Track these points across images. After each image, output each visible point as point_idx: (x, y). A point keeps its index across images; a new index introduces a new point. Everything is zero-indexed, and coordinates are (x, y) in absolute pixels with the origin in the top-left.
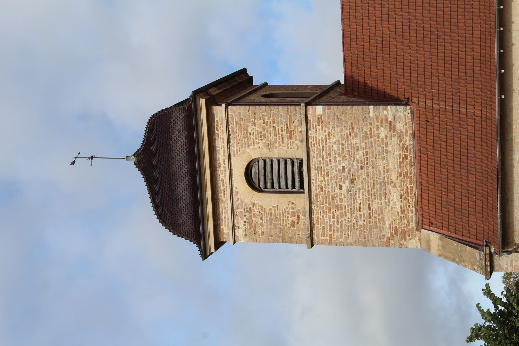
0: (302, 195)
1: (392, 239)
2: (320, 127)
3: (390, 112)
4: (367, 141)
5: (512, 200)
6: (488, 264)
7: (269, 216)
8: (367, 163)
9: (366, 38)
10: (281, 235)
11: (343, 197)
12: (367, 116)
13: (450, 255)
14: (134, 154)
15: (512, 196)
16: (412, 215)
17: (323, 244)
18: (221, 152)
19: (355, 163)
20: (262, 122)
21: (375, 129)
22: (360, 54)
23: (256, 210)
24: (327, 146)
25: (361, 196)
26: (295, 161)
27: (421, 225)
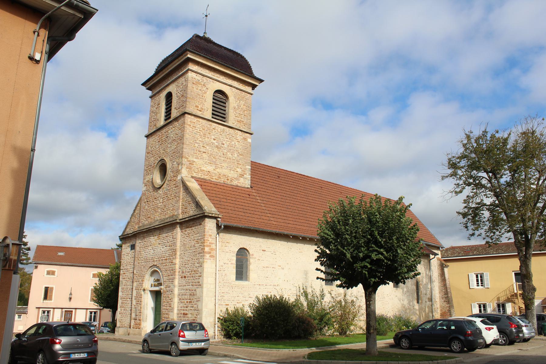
2: (242, 138)
3: (248, 176)
4: (235, 161)
5: (241, 235)
6: (213, 215)
7: (201, 95)
11: (210, 139)
12: (246, 164)
15: (243, 235)
18: (232, 83)
20: (245, 110)
23: (205, 89)
25: (210, 149)
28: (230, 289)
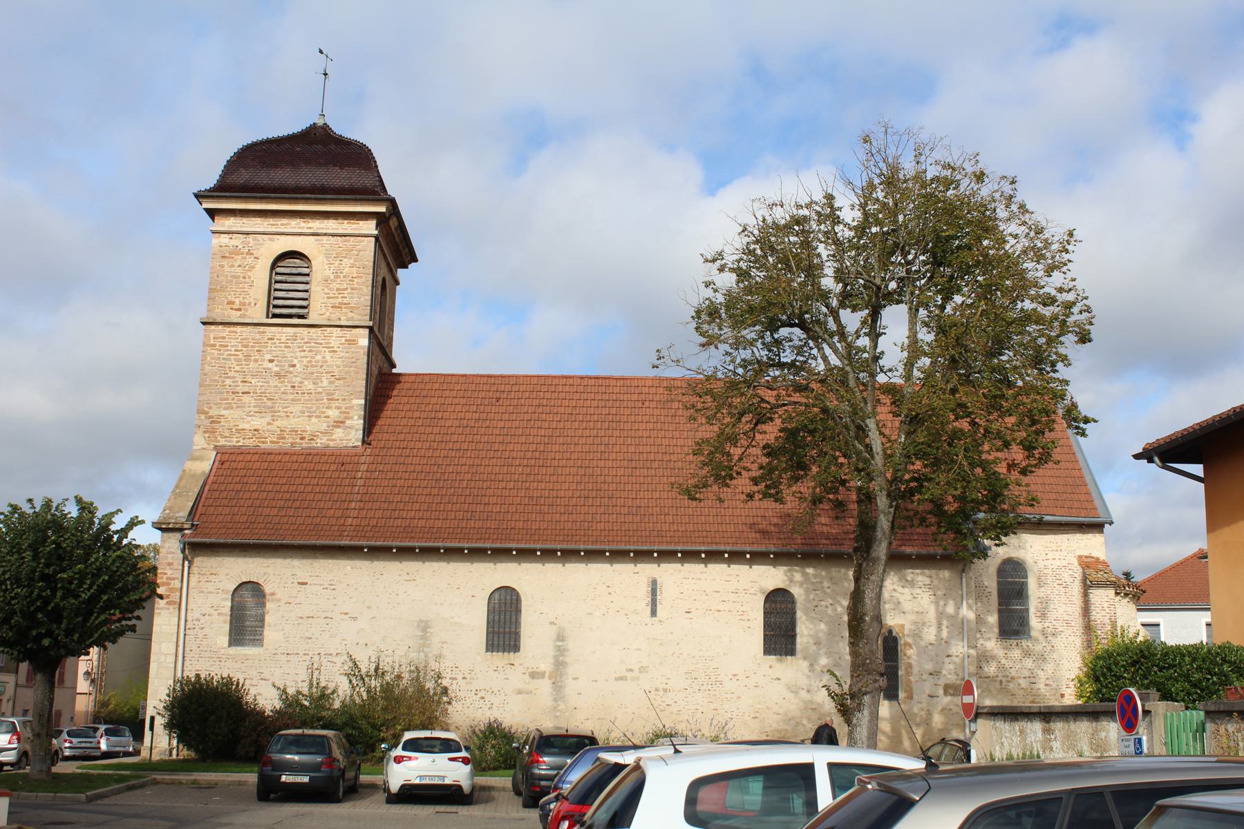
0: (265, 315)
1: (206, 417)
3: (356, 422)
5: (245, 556)
6: (171, 526)
7: (242, 275)
8: (298, 393)
9: (441, 401)
10: (218, 288)
12: (352, 397)
13: (183, 482)
14: (326, 124)
15: (250, 557)
16: (234, 442)
17: (205, 336)
18: (322, 225)
19: (298, 379)
20: (354, 276)
21: (337, 405)
22: (425, 393)
23: (250, 260)
24: (321, 349)
26: (306, 311)
27: (220, 451)
28: (213, 663)
